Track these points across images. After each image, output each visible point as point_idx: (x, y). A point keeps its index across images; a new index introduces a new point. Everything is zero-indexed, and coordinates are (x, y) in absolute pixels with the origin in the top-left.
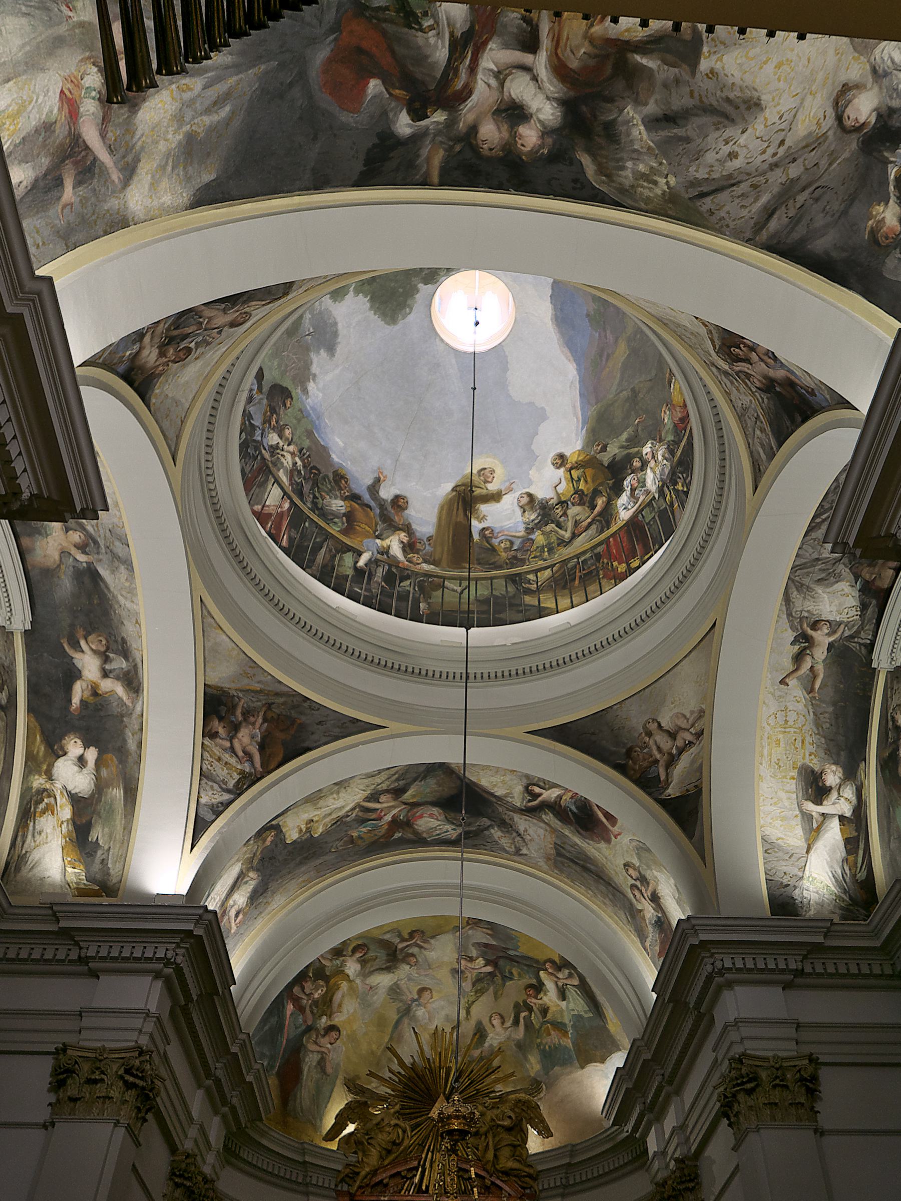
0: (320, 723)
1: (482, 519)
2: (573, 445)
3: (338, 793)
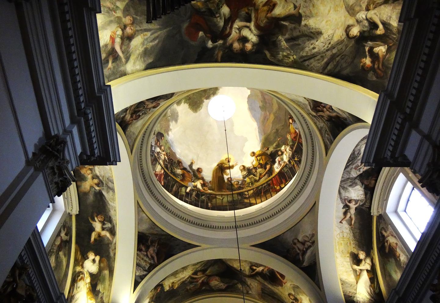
0: (177, 245)
1: (227, 175)
2: (257, 148)
3: (183, 272)
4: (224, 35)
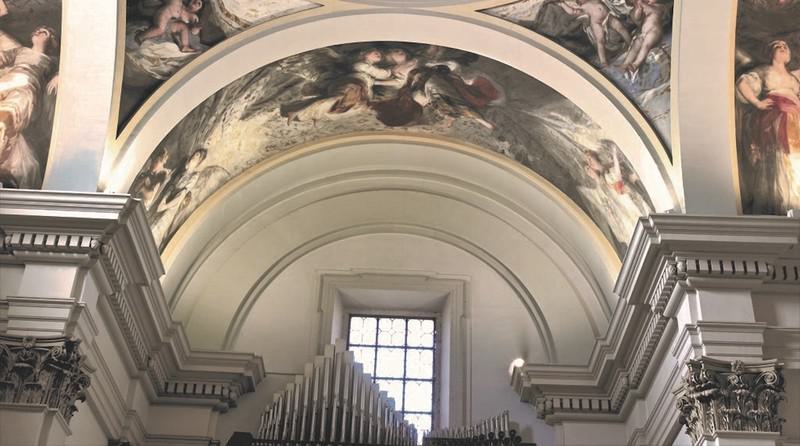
4: (425, 73)
